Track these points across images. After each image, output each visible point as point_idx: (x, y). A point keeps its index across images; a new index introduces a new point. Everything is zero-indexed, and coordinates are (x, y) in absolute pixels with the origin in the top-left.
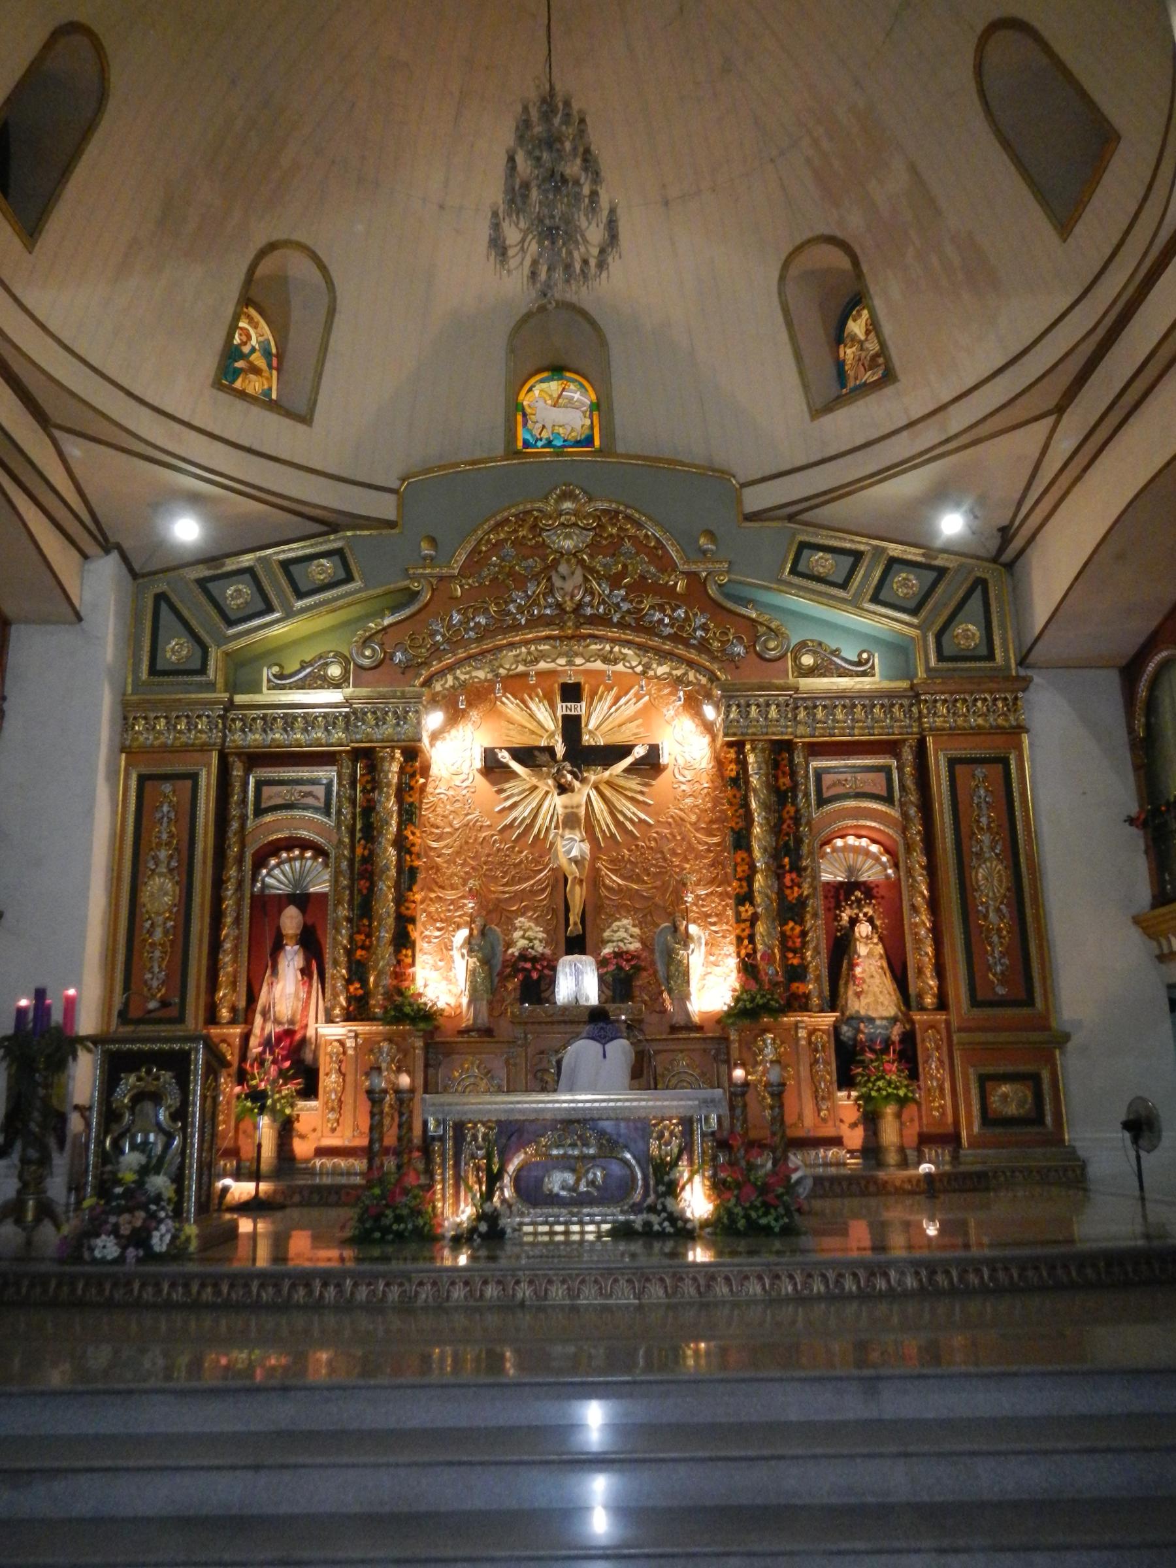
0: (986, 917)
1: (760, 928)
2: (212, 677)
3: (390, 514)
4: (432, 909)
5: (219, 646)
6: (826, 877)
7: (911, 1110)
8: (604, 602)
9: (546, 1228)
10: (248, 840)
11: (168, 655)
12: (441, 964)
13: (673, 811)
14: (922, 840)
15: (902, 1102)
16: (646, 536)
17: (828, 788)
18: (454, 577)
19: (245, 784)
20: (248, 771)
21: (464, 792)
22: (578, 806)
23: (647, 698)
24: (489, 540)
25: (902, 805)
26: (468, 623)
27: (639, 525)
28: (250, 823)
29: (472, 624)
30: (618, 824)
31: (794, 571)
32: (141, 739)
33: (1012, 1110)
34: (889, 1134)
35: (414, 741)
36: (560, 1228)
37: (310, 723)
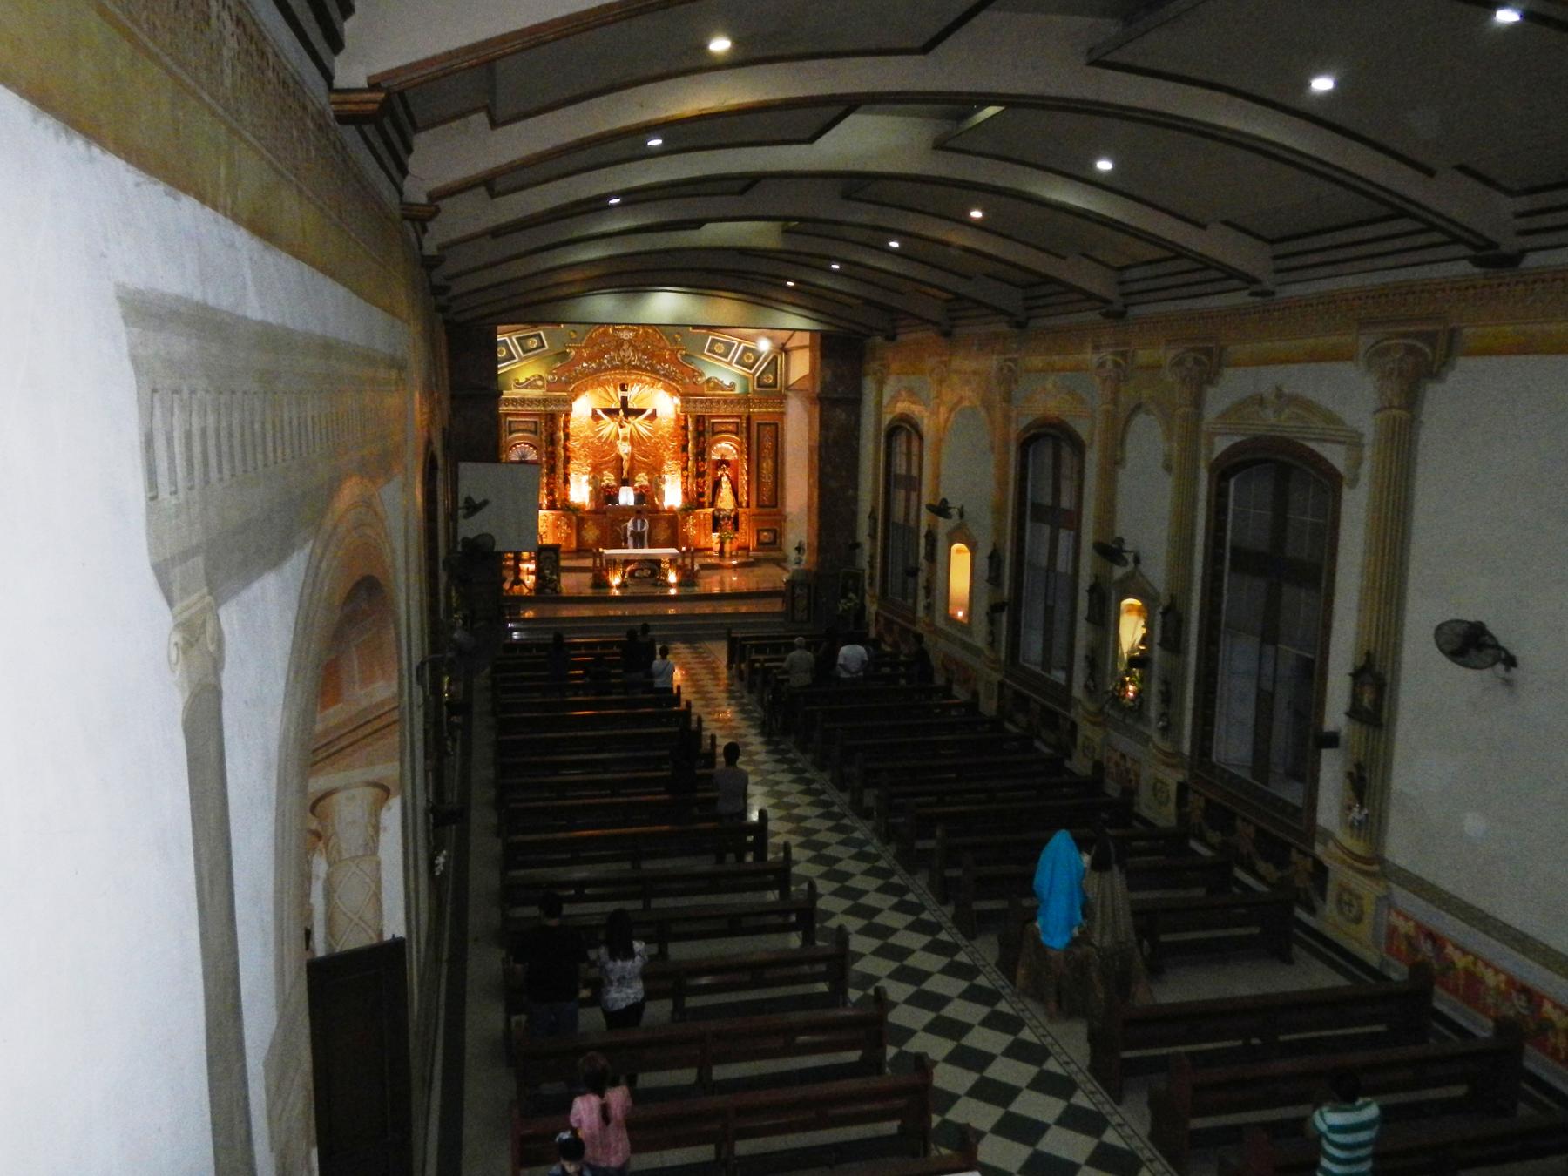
1: (690, 480)
6: (713, 457)
7: (734, 540)
13: (660, 433)
15: (731, 539)
31: (709, 351)
33: (767, 540)
34: (727, 547)
37: (531, 402)
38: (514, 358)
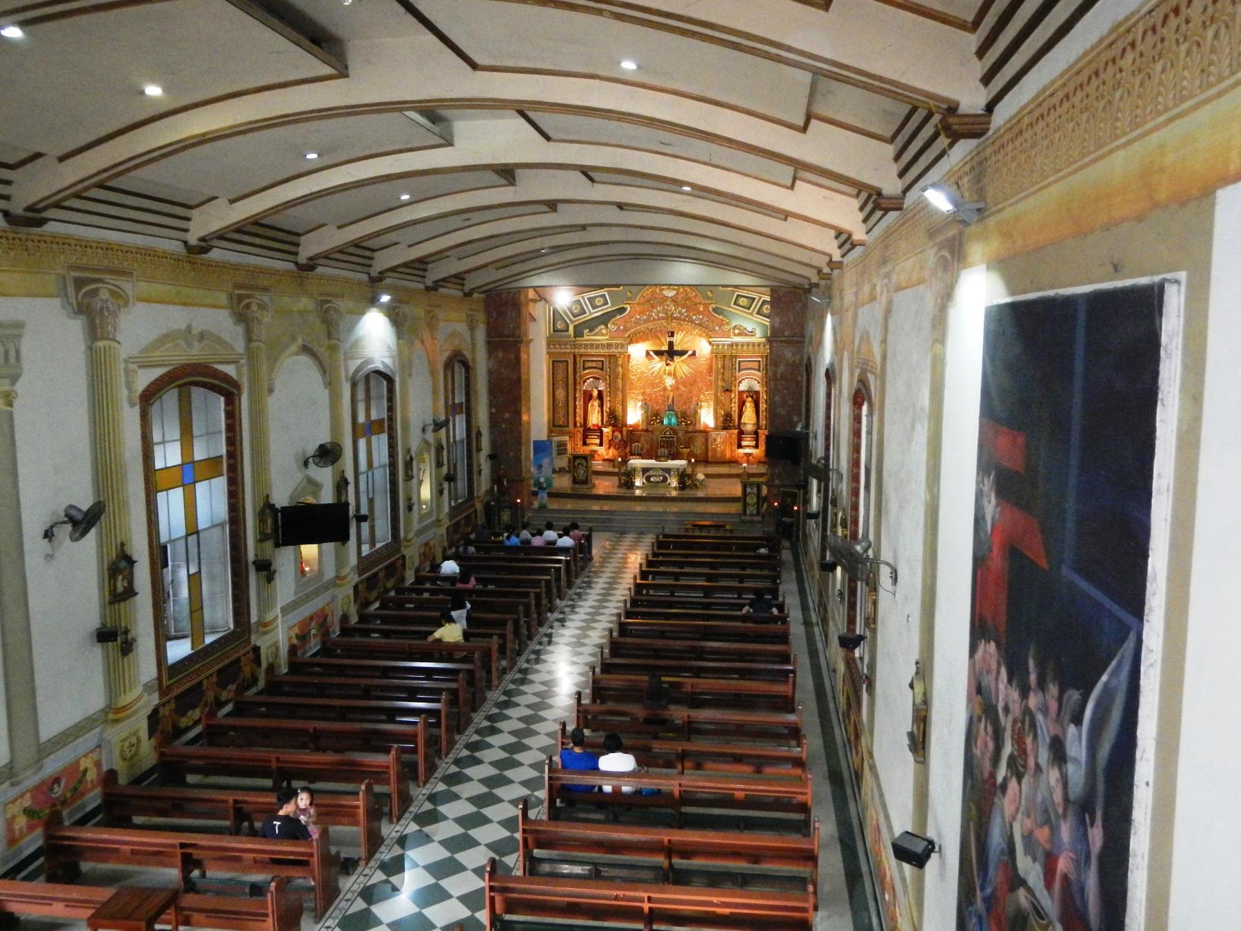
31: (735, 304)
38: (585, 313)
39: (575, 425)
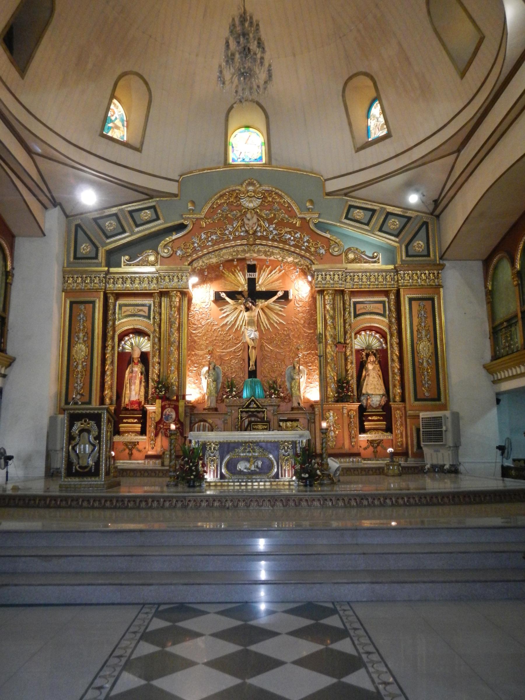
0: (422, 364)
2: (100, 260)
3: (175, 191)
4: (193, 359)
5: (103, 247)
8: (266, 230)
9: (238, 484)
10: (117, 328)
11: (82, 250)
12: (197, 381)
14: (397, 332)
16: (284, 202)
17: (359, 310)
18: (202, 219)
19: (115, 306)
20: (116, 300)
21: (206, 310)
22: (255, 316)
23: (284, 271)
24: (217, 203)
25: (389, 317)
26: (208, 238)
27: (281, 197)
28: (117, 323)
29: (210, 239)
30: (271, 324)
32: (71, 286)
35: (185, 288)
36: (244, 484)
39: (102, 401)
